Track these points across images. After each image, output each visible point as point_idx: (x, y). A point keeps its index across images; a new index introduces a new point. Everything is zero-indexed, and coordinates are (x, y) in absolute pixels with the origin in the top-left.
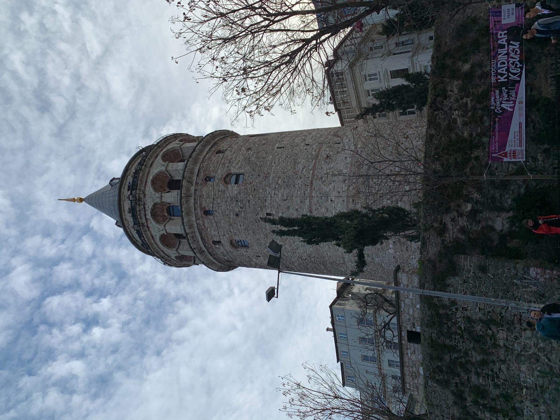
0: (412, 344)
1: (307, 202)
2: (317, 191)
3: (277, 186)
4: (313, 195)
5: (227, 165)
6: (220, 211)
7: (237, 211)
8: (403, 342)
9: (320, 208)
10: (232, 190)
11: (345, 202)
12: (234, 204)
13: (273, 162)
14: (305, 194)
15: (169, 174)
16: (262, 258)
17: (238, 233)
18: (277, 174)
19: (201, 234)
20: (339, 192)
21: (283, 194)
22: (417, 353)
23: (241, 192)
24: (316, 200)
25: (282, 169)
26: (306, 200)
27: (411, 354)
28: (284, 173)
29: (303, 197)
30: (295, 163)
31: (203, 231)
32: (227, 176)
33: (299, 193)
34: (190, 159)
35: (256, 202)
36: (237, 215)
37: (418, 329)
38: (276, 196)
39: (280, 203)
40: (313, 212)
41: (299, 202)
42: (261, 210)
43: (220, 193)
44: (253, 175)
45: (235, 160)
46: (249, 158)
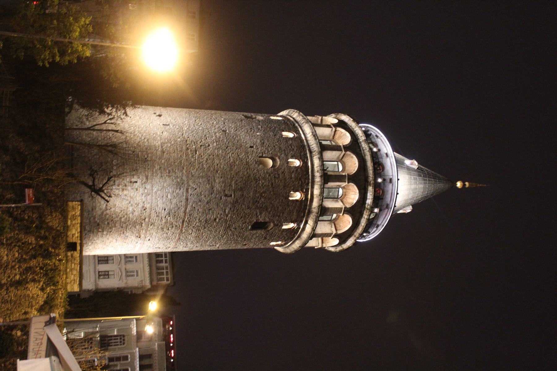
0: (74, 241)
4: (182, 214)
16: (248, 145)
43: (278, 214)
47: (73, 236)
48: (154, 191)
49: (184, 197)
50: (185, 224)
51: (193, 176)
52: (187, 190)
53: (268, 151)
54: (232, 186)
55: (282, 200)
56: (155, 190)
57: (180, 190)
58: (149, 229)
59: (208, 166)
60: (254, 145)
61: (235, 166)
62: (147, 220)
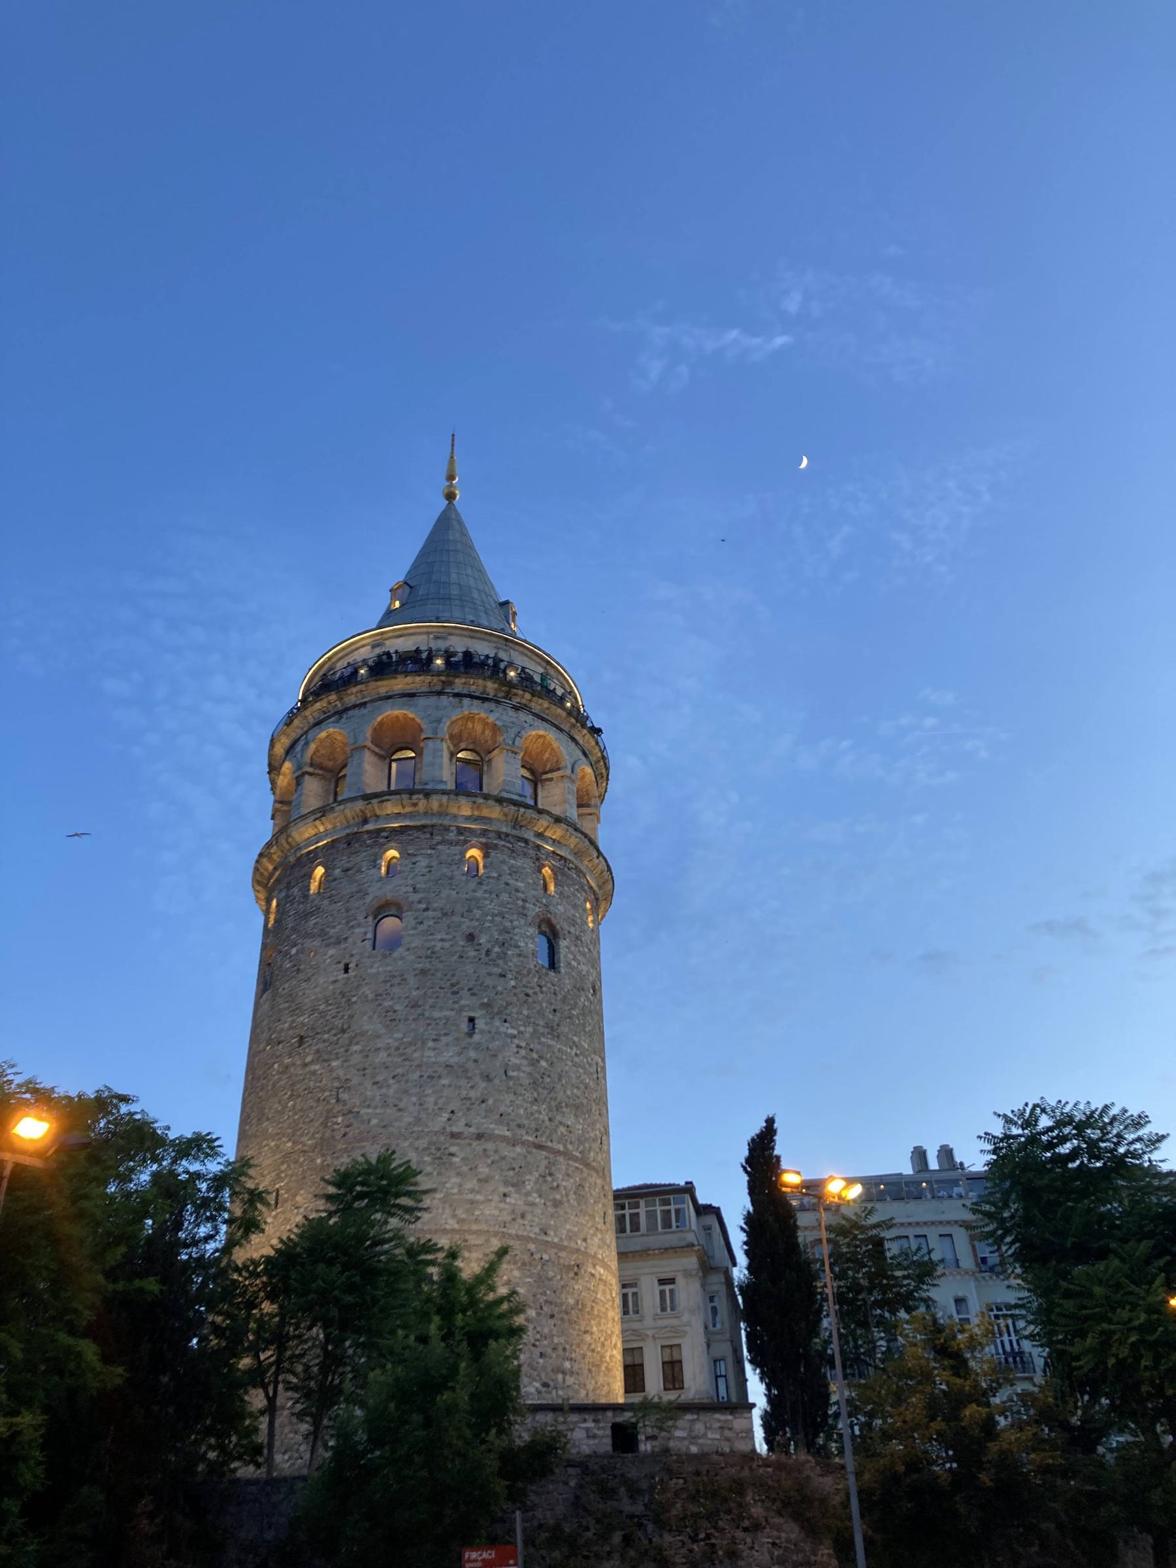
0: (609, 1432)
1: (502, 1131)
2: (525, 1157)
3: (535, 1056)
4: (518, 1149)
5: (572, 930)
6: (479, 894)
7: (481, 941)
8: (610, 1414)
9: (489, 1161)
10: (528, 937)
11: (505, 1230)
12: (496, 934)
13: (578, 1052)
14: (519, 1126)
15: (551, 779)
16: (342, 976)
17: (421, 927)
18: (557, 1058)
19: (422, 828)
20: (523, 1216)
21: (518, 1068)
22: (591, 1442)
23: (521, 959)
24: (506, 1153)
25: (567, 1072)
26: (506, 1128)
27: (587, 1430)
28: (560, 1077)
29: (513, 1120)
30: (577, 1107)
31: (428, 836)
32: (552, 927)
33: (522, 1111)
34: (587, 842)
35: (501, 994)
36: (471, 938)
37: (645, 1447)
38: (515, 1050)
39: (500, 1057)
40: (478, 1142)
41: (502, 1109)
42: (484, 1006)
43: (520, 903)
44: (555, 994)
45: (579, 951)
46: (583, 990)
47: (595, 1436)
48: (456, 1226)
49: (474, 1143)
50: (542, 1140)
51: (418, 1120)
52: (453, 1135)
53: (359, 925)
54: (447, 1019)
55: (485, 891)
56: (452, 1224)
57: (452, 1155)
58: (556, 1240)
59: (391, 1081)
60: (339, 962)
61: (395, 1011)
62: (532, 1247)
